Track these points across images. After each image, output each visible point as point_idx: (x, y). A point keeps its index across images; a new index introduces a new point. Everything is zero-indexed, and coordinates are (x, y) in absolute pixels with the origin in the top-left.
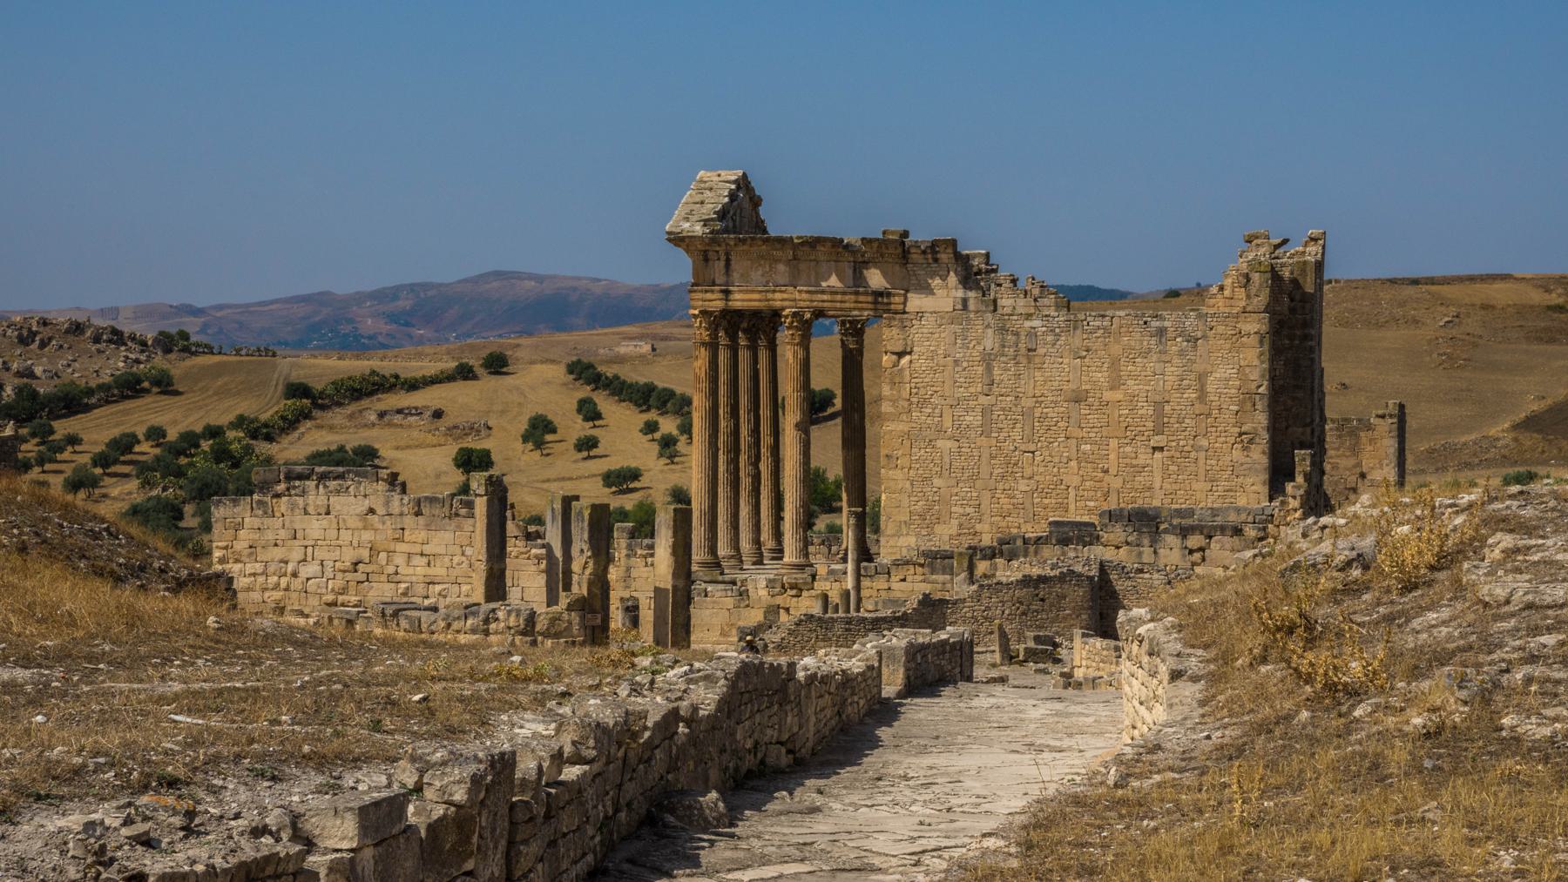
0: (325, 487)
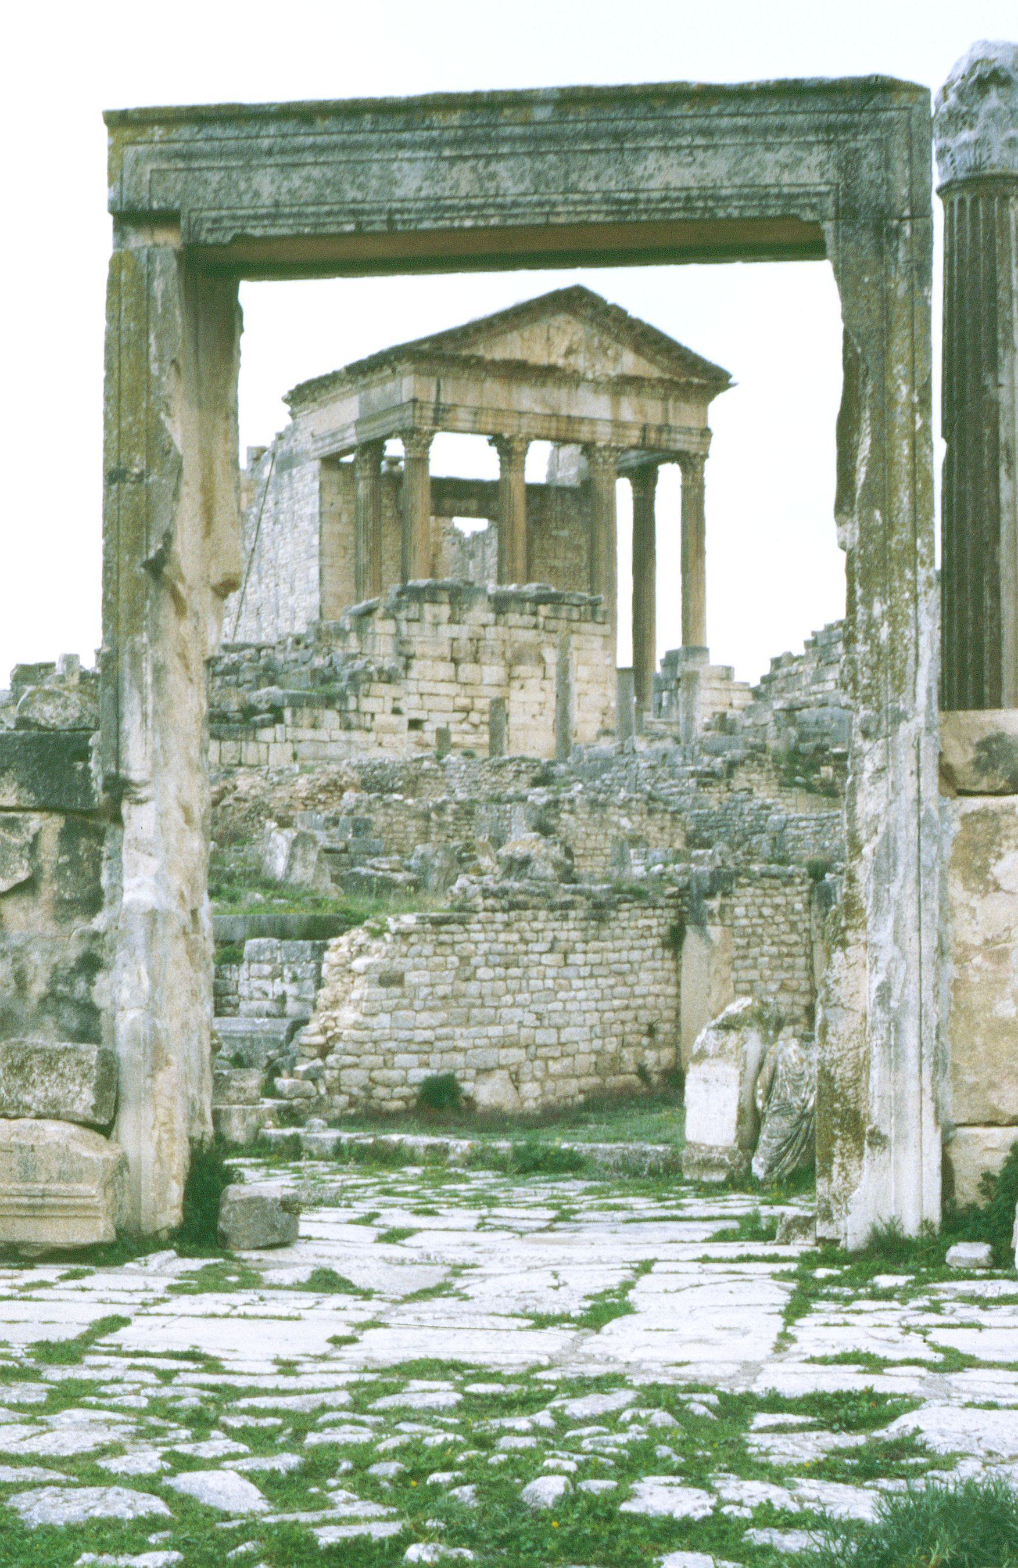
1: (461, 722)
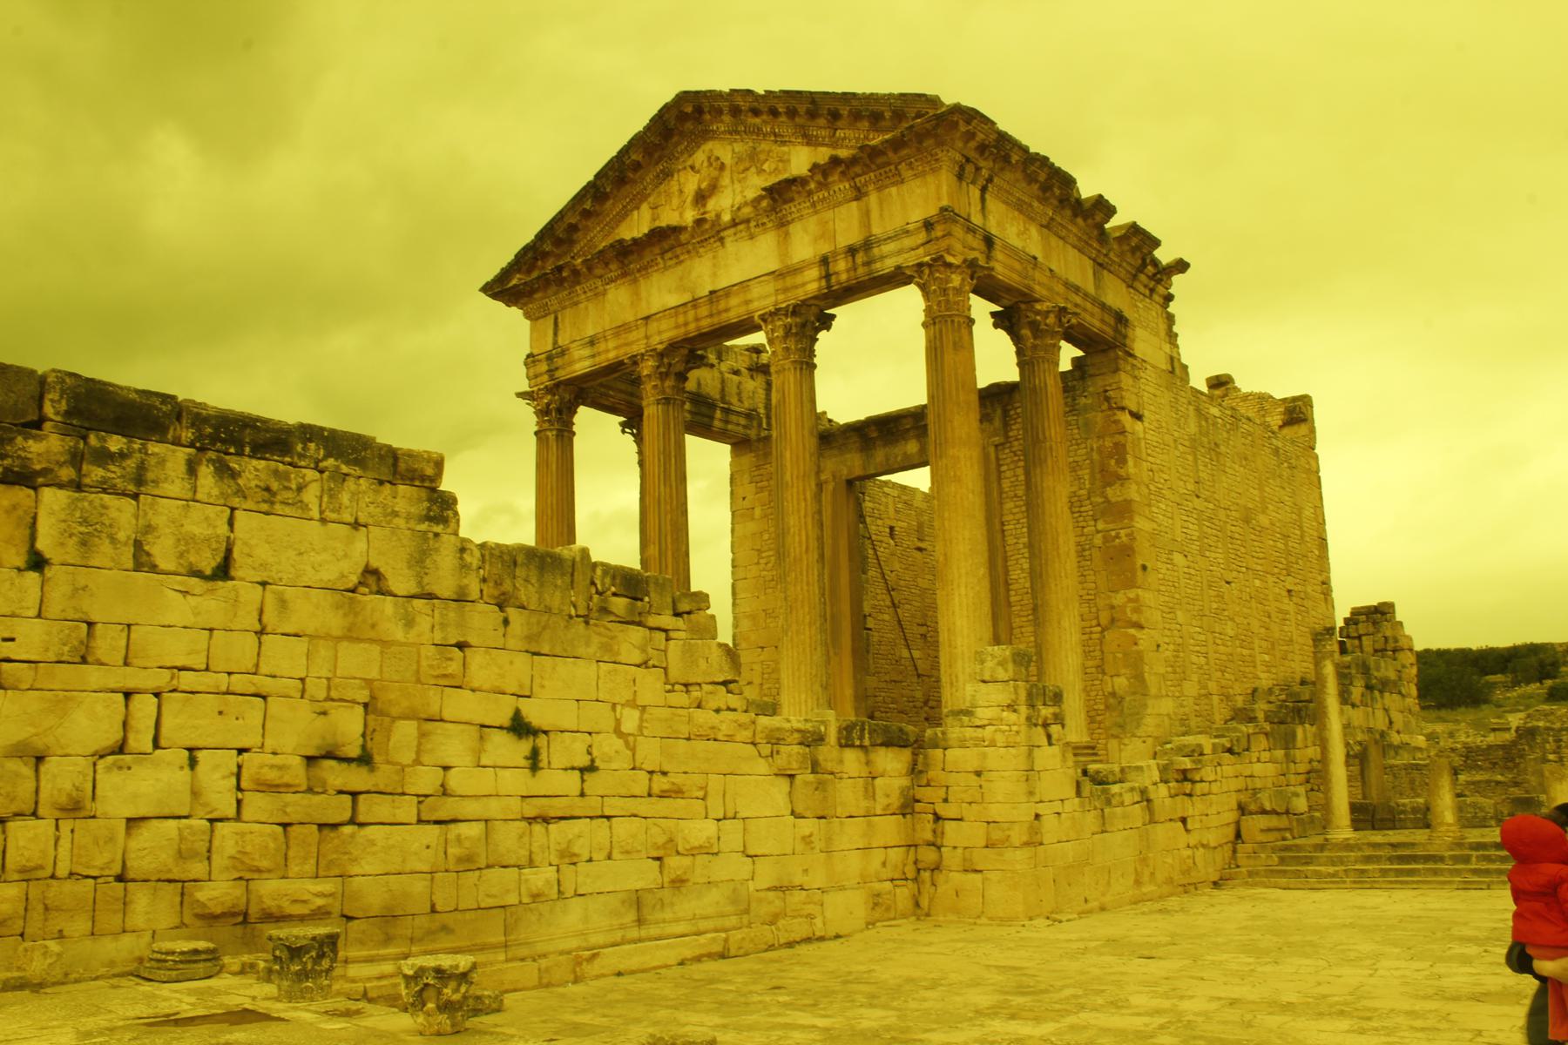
0: (224, 471)
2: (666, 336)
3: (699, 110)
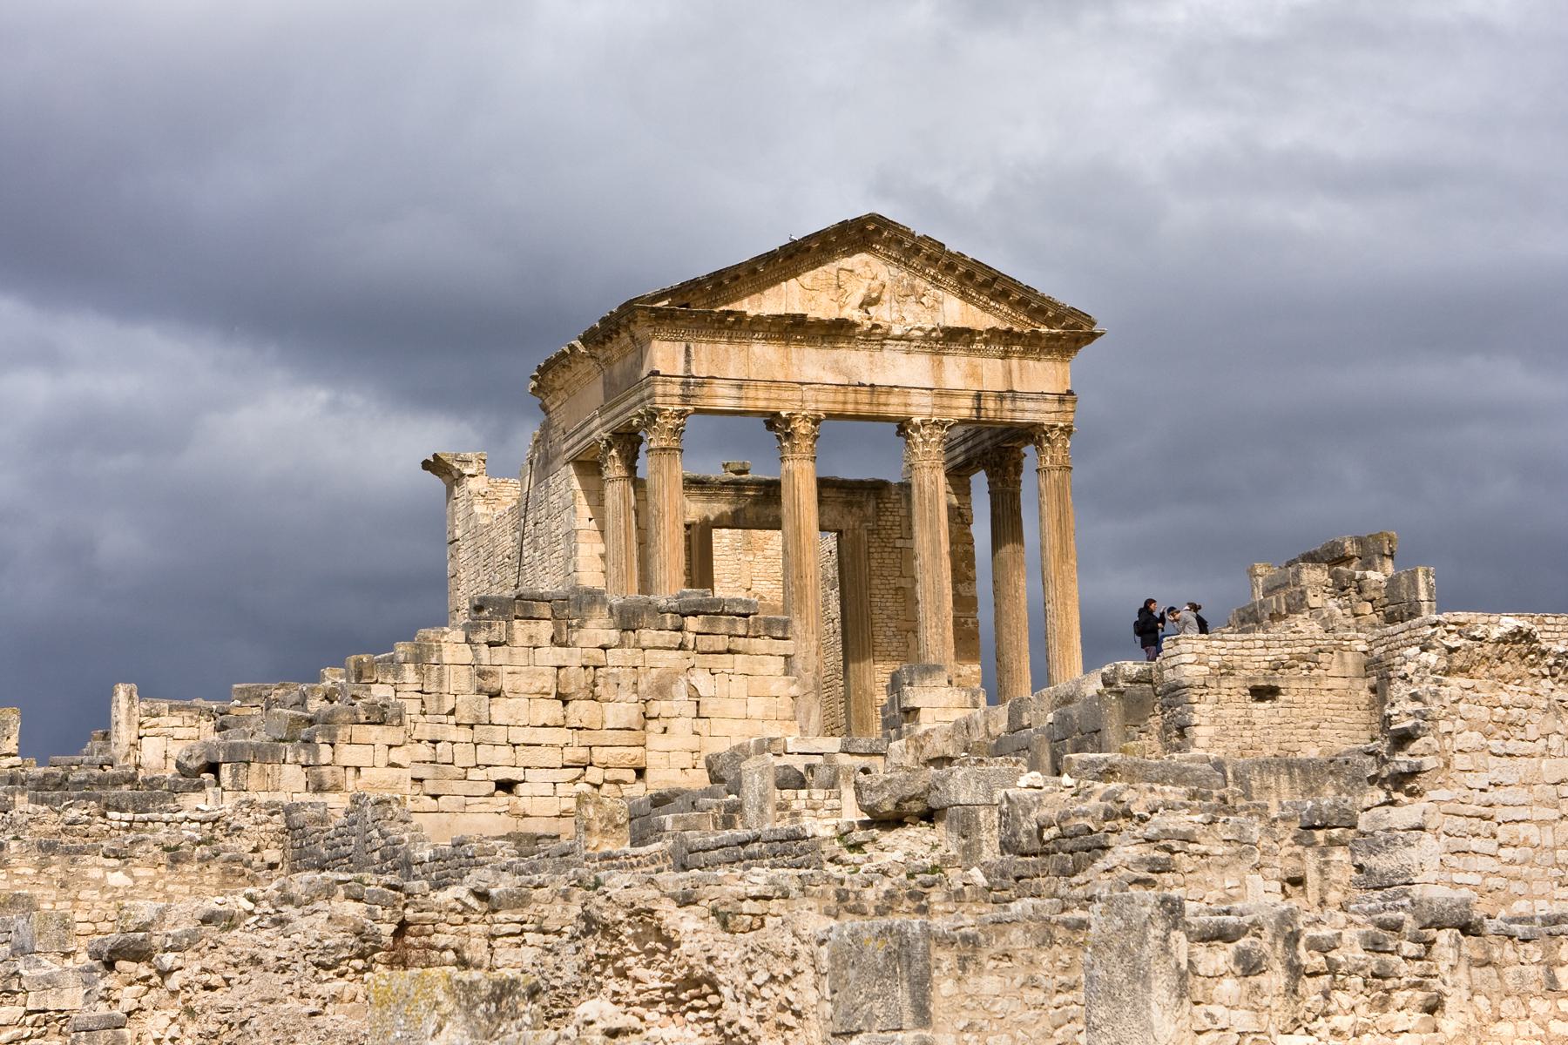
1: (574, 781)
2: (820, 406)
3: (878, 231)
